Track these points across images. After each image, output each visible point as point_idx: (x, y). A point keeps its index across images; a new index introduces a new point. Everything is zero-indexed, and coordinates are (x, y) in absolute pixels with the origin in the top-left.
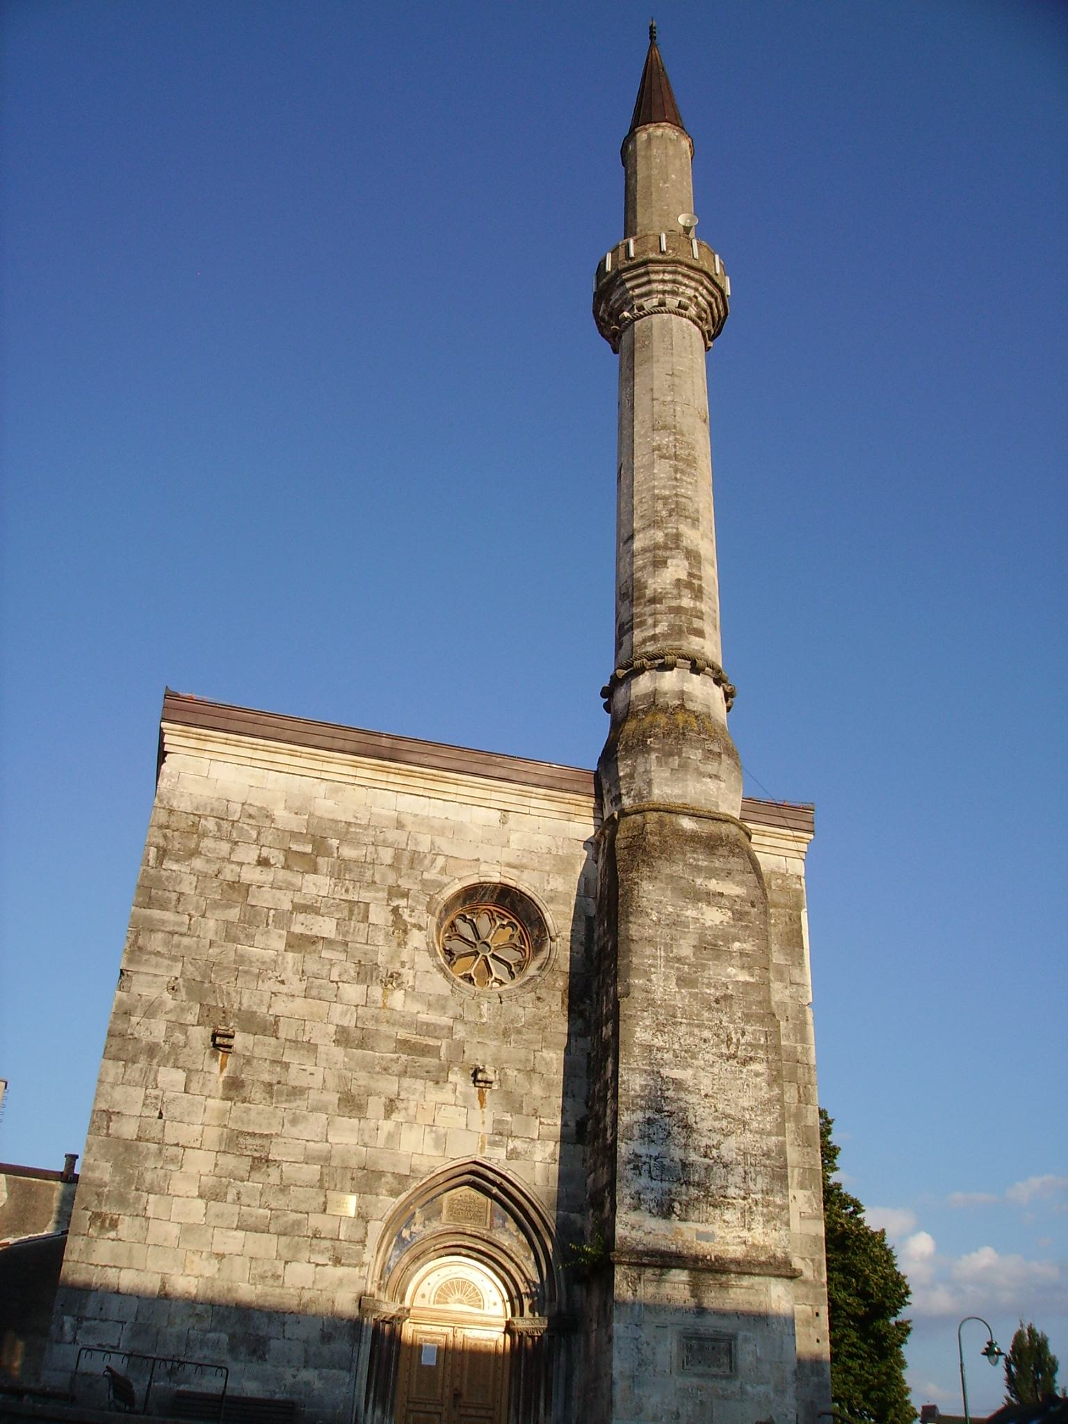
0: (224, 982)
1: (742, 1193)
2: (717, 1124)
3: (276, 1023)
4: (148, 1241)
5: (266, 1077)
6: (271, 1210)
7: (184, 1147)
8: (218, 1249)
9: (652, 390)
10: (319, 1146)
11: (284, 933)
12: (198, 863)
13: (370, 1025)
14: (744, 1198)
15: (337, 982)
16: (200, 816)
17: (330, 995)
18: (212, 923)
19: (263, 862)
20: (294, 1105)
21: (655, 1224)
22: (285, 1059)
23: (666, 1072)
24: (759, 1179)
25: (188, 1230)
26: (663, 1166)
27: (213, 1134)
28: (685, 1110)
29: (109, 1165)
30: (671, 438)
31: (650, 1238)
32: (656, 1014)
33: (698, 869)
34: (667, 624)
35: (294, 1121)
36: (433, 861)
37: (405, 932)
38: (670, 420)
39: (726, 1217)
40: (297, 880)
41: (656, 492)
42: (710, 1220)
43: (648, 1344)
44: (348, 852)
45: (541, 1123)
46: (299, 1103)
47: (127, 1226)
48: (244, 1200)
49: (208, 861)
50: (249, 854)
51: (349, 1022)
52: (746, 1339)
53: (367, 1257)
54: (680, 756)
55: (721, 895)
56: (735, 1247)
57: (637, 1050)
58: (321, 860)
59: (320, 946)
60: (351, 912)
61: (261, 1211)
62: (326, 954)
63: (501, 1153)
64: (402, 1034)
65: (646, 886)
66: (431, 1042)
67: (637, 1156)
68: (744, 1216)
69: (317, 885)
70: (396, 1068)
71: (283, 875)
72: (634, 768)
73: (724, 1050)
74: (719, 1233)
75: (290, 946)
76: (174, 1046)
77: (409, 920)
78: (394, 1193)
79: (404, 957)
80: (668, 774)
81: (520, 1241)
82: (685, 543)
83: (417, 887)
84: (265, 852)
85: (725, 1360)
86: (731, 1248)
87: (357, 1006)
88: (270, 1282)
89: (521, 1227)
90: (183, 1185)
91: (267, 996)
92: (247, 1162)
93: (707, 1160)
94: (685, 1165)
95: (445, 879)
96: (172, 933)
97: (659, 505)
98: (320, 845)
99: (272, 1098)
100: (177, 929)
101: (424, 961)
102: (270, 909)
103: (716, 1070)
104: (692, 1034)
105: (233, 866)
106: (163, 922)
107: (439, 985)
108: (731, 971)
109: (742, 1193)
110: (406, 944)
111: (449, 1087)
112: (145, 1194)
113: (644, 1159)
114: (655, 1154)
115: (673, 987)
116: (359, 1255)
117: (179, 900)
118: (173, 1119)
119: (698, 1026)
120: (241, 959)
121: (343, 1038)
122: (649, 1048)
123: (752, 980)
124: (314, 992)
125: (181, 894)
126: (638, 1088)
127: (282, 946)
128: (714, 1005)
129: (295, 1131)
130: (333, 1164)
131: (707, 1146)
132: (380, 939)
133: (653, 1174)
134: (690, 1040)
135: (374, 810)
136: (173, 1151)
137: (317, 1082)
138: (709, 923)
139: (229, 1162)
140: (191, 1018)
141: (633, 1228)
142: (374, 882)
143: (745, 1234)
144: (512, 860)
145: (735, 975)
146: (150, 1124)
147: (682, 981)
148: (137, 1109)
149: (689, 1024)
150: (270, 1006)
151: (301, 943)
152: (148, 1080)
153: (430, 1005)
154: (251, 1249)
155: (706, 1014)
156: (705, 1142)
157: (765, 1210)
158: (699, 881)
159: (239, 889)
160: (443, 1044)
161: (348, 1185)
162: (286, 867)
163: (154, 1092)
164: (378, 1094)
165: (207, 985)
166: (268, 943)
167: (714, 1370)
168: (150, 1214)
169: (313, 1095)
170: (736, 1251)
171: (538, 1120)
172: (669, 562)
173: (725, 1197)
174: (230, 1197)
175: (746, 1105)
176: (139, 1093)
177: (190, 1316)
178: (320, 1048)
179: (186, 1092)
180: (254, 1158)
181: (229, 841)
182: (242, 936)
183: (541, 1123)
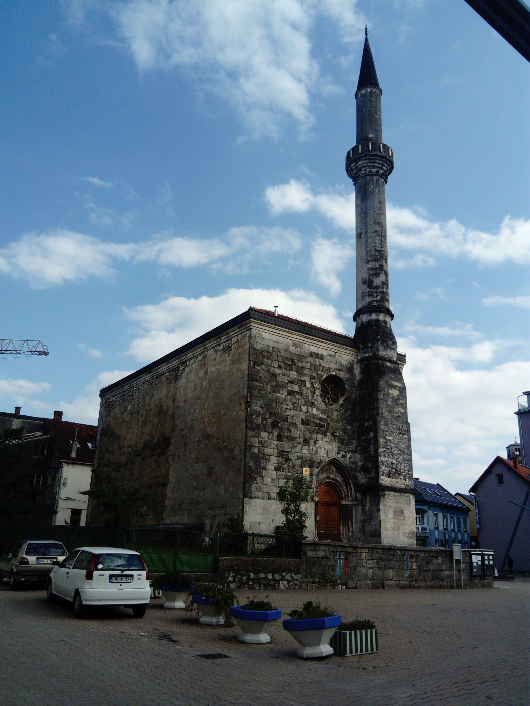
0: (274, 404)
3: (287, 418)
4: (264, 484)
5: (286, 434)
6: (291, 473)
7: (270, 456)
9: (374, 207)
10: (300, 454)
11: (287, 390)
12: (263, 367)
13: (309, 418)
14: (404, 472)
15: (300, 405)
16: (262, 351)
17: (299, 409)
18: (269, 386)
19: (280, 367)
20: (294, 442)
21: (387, 479)
22: (290, 429)
23: (387, 438)
25: (273, 479)
26: (388, 463)
27: (276, 451)
28: (391, 448)
29: (252, 461)
30: (380, 228)
31: (386, 483)
32: (385, 420)
33: (392, 379)
34: (380, 297)
35: (294, 447)
36: (320, 368)
37: (315, 390)
38: (379, 221)
39: (401, 478)
40: (288, 373)
41: (376, 248)
44: (300, 365)
45: (348, 447)
46: (294, 442)
47: (259, 479)
48: (285, 470)
49: (266, 366)
50: (275, 364)
51: (304, 417)
53: (313, 486)
54: (387, 343)
55: (397, 386)
57: (381, 432)
58: (293, 367)
59: (295, 394)
60: (302, 384)
61: (289, 473)
62: (297, 397)
63: (340, 456)
64: (316, 421)
65: (381, 383)
66: (323, 423)
67: (383, 461)
68: (404, 477)
69: (293, 375)
70: (315, 431)
71: (285, 371)
72: (373, 345)
73: (399, 432)
74: (400, 482)
75: (289, 394)
76: (264, 425)
77: (315, 386)
78: (318, 468)
79: (315, 398)
80: (383, 348)
81: (342, 480)
82: (384, 268)
83: (316, 376)
84: (280, 363)
85: (402, 515)
87: (305, 413)
89: (342, 476)
90: (271, 467)
91: (284, 409)
94: (392, 463)
95: (323, 373)
96: (260, 390)
97: (377, 253)
98: (292, 361)
99: (288, 440)
101: (320, 399)
102: (282, 382)
103: (397, 437)
104: (392, 426)
105: (272, 368)
106: (257, 386)
107: (323, 406)
108: (400, 409)
110: (315, 394)
111: (328, 437)
112: (262, 470)
113: (384, 462)
114: (386, 460)
115: (388, 413)
116: (311, 485)
117: (260, 379)
118: (266, 447)
119: (393, 425)
120: (277, 398)
121: (304, 422)
122: (383, 430)
123: (404, 411)
124: (295, 408)
126: (382, 442)
127: (286, 394)
129: (294, 450)
131: (396, 458)
132: (309, 392)
134: (391, 429)
135: (305, 351)
136: (267, 456)
137: (298, 435)
138: (395, 395)
139: (280, 459)
140: (267, 416)
142: (306, 374)
143: (405, 482)
144: (338, 368)
145: (401, 410)
146: (261, 449)
147: (390, 412)
148: (257, 445)
149: (391, 424)
150: (285, 413)
151: (291, 393)
152: (259, 436)
153: (322, 413)
155: (395, 421)
156: (396, 457)
158: (392, 382)
159: (274, 375)
160: (325, 424)
161: (307, 465)
162: (285, 369)
164: (312, 439)
165: (270, 406)
166: (283, 393)
167: (400, 518)
168: (263, 476)
169: (298, 439)
170: (403, 486)
171: (347, 447)
172: (380, 275)
173: (400, 472)
174: (281, 470)
175: (404, 447)
176: (257, 440)
177: (276, 504)
178: (298, 425)
179: (268, 439)
181: (271, 360)
182: (277, 391)
183: (348, 447)
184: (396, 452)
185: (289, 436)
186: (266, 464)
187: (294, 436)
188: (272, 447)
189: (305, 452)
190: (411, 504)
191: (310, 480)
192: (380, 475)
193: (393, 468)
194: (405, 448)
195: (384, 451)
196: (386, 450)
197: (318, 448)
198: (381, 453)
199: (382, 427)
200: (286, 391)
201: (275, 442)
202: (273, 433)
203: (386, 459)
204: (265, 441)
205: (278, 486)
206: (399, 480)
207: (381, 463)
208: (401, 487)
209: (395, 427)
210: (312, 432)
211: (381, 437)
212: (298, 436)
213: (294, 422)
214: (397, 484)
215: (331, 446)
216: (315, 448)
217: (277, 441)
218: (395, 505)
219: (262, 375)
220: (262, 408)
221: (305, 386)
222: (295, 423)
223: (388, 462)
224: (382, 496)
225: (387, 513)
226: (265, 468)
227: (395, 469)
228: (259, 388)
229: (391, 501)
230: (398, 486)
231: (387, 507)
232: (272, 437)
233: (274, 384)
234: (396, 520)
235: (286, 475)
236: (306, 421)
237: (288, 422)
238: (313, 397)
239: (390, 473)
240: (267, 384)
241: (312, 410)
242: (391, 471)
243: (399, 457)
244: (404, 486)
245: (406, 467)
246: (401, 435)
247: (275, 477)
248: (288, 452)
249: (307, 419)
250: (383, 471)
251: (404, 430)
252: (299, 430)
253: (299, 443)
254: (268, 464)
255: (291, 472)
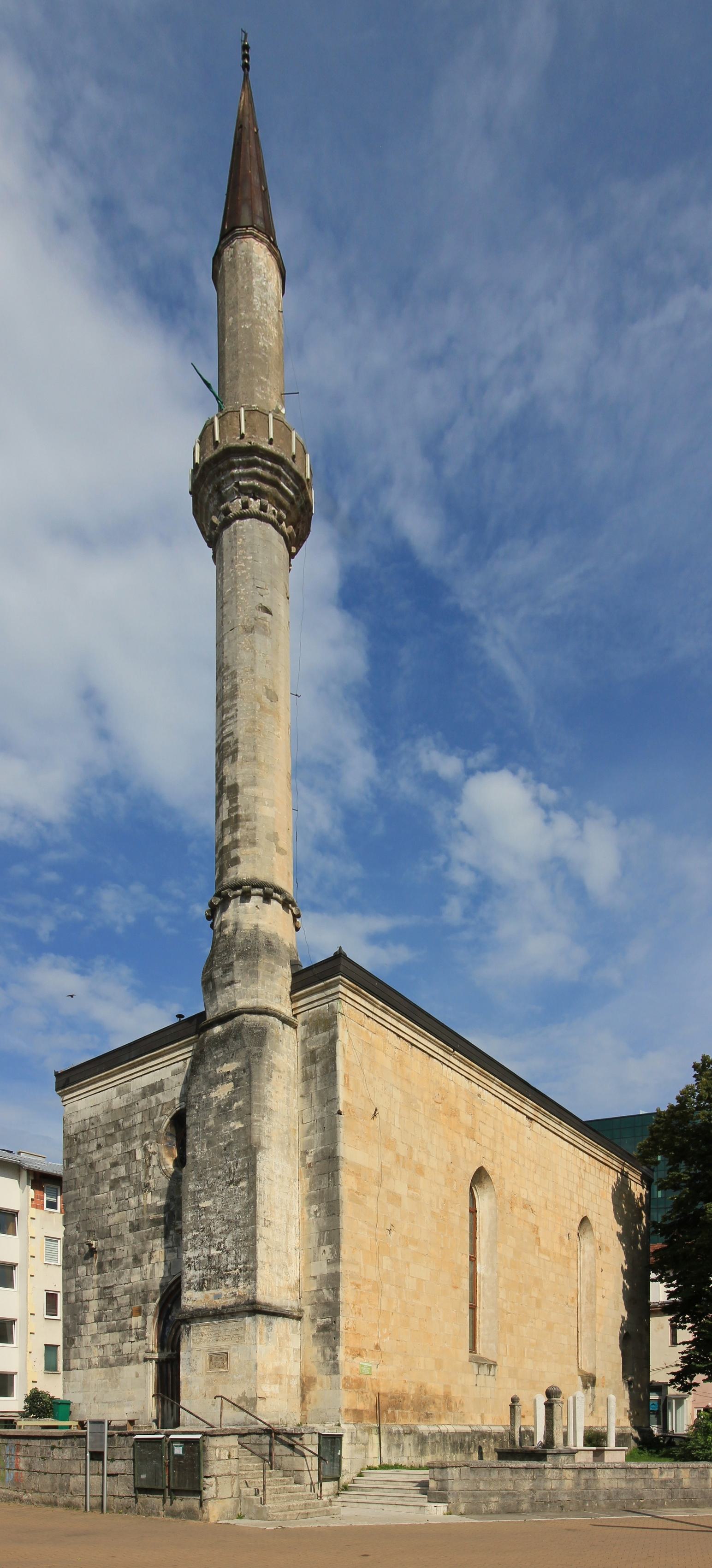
0: (93, 1216)
1: (234, 1266)
2: (224, 1228)
6: (116, 1320)
8: (102, 1343)
15: (127, 1199)
17: (125, 1207)
20: (119, 1268)
21: (198, 1295)
24: (243, 1256)
25: (94, 1337)
26: (200, 1261)
27: (96, 1291)
31: (195, 1303)
35: (120, 1277)
39: (227, 1283)
42: (220, 1286)
43: (194, 1360)
52: (234, 1350)
56: (230, 1299)
64: (152, 1216)
67: (189, 1259)
68: (234, 1280)
70: (151, 1235)
73: (228, 1180)
74: (224, 1293)
78: (154, 1300)
86: (229, 1300)
88: (119, 1354)
90: (90, 1318)
92: (107, 1300)
93: (220, 1252)
100: (76, 1198)
109: (234, 1266)
113: (192, 1260)
116: (144, 1333)
120: (97, 1201)
125: (76, 1178)
127: (107, 1189)
128: (224, 1152)
130: (133, 1292)
133: (196, 1267)
134: (212, 1180)
139: (102, 1302)
141: (188, 1300)
143: (235, 1290)
150: (107, 1222)
154: (113, 1341)
156: (219, 1240)
157: (245, 1273)
163: (77, 1279)
168: (82, 1334)
169: (124, 1261)
170: (231, 1301)
173: (226, 1271)
178: (125, 1236)
180: (109, 1298)
184: (219, 1230)
185: (113, 1259)
186: (85, 1316)
187: (120, 1257)
188: (91, 1287)
189: (136, 1278)
190: (246, 1337)
191: (144, 1325)
192: (184, 1290)
193: (211, 1268)
194: (239, 1213)
195: (195, 1237)
196: (197, 1233)
197: (156, 1264)
198: (187, 1243)
199: (191, 1187)
200: (108, 1183)
201: (95, 1277)
202: (92, 1263)
203: (196, 1254)
204: (83, 1280)
205: (100, 1346)
206: (222, 1291)
207: (187, 1265)
208: (225, 1305)
209: (220, 1173)
210: (145, 1239)
211: (187, 1209)
212: (125, 1255)
213: (120, 1233)
214: (217, 1301)
215: (176, 1254)
216: (149, 1266)
217: (98, 1274)
218: (212, 1345)
219: (78, 1176)
220: (78, 1228)
221: (135, 1159)
222: (121, 1235)
223: (201, 1258)
224: (184, 1332)
225: (193, 1365)
226: (84, 1323)
227: (214, 1268)
228: (74, 1199)
229: (204, 1338)
230: (219, 1303)
231: (194, 1352)
232: (91, 1269)
233: (93, 1180)
234: (212, 1376)
235: (110, 1325)
236: (136, 1223)
237: (111, 1237)
238: (147, 1174)
239: (204, 1280)
240: (83, 1187)
241: (145, 1199)
242: (207, 1275)
243: (225, 1239)
244: (234, 1298)
245: (240, 1257)
246: (232, 1186)
247: (95, 1332)
248: (112, 1287)
249: (138, 1220)
250: (190, 1280)
251: (240, 1171)
252: (126, 1244)
253: (127, 1267)
254: (88, 1314)
255: (116, 1318)
